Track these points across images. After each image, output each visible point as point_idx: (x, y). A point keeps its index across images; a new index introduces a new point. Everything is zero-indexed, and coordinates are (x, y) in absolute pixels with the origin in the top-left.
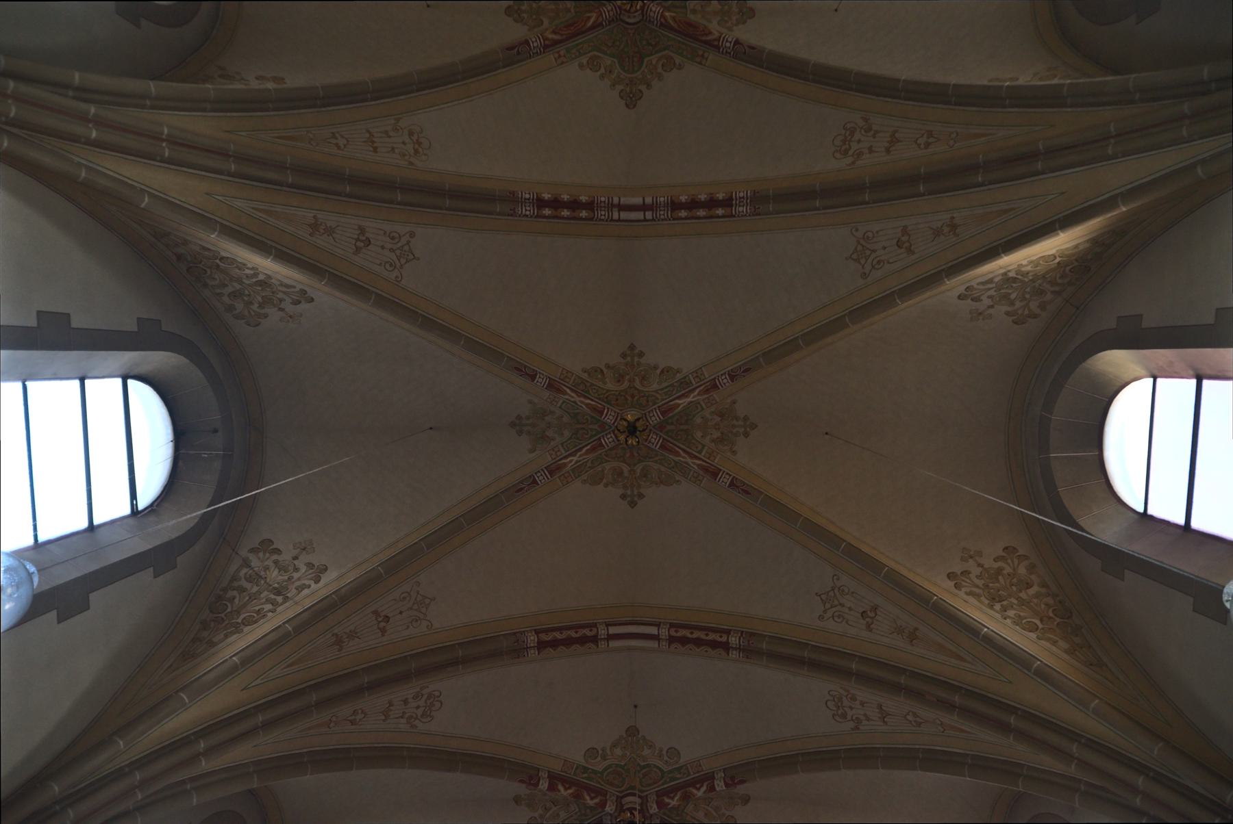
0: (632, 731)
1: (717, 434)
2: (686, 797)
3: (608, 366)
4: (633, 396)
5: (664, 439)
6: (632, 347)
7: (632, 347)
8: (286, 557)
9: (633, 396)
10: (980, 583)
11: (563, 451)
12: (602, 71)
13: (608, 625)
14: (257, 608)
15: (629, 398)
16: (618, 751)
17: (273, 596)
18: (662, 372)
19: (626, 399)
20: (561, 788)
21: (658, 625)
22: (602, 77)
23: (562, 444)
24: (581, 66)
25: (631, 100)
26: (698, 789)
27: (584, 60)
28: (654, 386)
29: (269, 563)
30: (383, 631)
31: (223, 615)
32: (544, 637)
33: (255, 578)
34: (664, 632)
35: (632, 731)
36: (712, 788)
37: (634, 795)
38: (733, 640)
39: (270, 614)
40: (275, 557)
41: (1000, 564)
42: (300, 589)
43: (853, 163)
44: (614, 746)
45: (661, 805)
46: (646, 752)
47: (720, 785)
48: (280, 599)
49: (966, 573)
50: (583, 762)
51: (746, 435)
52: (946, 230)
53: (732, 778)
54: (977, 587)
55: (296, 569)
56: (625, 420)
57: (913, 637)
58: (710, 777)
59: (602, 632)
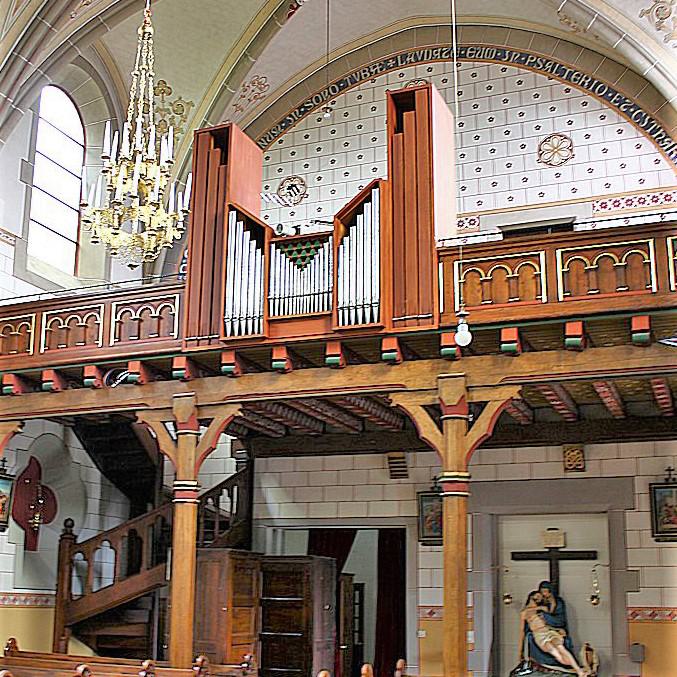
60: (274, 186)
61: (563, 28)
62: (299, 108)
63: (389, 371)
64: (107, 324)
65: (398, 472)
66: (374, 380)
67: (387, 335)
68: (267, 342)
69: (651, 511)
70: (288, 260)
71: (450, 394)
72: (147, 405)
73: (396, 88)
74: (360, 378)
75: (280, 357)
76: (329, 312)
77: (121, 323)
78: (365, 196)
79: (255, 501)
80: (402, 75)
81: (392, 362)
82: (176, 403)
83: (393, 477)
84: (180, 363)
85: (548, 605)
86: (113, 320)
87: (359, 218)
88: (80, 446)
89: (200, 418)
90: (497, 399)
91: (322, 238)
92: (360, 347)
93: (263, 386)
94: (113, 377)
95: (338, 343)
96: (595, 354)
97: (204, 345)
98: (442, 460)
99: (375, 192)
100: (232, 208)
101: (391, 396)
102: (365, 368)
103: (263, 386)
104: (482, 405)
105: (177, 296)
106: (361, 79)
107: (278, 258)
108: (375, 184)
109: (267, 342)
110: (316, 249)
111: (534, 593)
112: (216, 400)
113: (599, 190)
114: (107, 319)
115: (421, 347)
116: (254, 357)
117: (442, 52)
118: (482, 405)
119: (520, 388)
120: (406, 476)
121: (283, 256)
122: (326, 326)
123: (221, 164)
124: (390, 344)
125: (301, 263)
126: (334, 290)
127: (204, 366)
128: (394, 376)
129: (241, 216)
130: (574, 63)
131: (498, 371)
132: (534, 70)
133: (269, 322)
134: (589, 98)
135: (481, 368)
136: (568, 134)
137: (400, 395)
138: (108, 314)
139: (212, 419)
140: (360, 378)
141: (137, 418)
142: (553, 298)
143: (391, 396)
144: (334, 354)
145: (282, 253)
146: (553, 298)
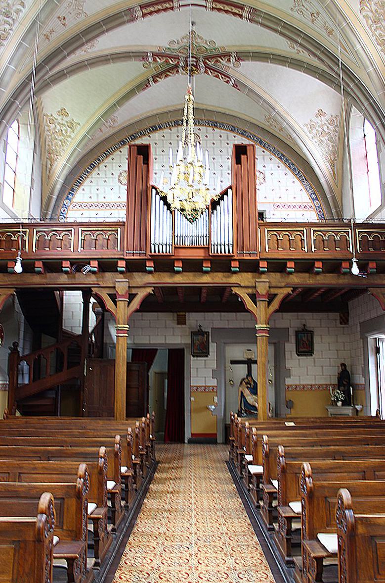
0: (193, 32)
2: (217, 61)
10: (374, 7)
16: (185, 40)
32: (145, 11)
34: (209, 5)
35: (193, 32)
36: (229, 60)
38: (245, 14)
45: (205, 63)
46: (199, 40)
47: (233, 60)
57: (330, 33)
59: (176, 5)
60: (117, 174)
61: (265, 123)
63: (232, 276)
64: (76, 239)
65: (181, 321)
66: (225, 280)
67: (235, 260)
69: (296, 344)
71: (262, 289)
72: (99, 284)
73: (239, 143)
74: (218, 279)
75: (178, 267)
76: (207, 246)
77: (84, 240)
78: (225, 193)
79: (105, 334)
82: (117, 285)
83: (178, 324)
84: (122, 265)
85: (250, 384)
88: (18, 302)
89: (130, 293)
90: (282, 293)
92: (222, 264)
93: (167, 279)
94: (79, 270)
95: (209, 262)
96: (325, 276)
98: (254, 319)
99: (230, 191)
100: (153, 187)
101: (232, 289)
102: (220, 275)
103: (167, 279)
104: (276, 295)
106: (164, 127)
108: (231, 187)
109: (173, 257)
111: (244, 379)
112: (140, 284)
113: (277, 200)
114: (76, 237)
115: (250, 267)
116: (164, 264)
118: (276, 295)
119: (292, 289)
120: (185, 324)
122: (205, 253)
124: (235, 265)
126: (210, 237)
127: (135, 267)
128: (234, 279)
131: (283, 280)
132: (249, 139)
133: (175, 248)
135: (275, 278)
137: (237, 288)
138: (76, 234)
139: (137, 294)
140: (218, 279)
141: (92, 291)
142: (310, 250)
144: (207, 267)
146: (310, 250)
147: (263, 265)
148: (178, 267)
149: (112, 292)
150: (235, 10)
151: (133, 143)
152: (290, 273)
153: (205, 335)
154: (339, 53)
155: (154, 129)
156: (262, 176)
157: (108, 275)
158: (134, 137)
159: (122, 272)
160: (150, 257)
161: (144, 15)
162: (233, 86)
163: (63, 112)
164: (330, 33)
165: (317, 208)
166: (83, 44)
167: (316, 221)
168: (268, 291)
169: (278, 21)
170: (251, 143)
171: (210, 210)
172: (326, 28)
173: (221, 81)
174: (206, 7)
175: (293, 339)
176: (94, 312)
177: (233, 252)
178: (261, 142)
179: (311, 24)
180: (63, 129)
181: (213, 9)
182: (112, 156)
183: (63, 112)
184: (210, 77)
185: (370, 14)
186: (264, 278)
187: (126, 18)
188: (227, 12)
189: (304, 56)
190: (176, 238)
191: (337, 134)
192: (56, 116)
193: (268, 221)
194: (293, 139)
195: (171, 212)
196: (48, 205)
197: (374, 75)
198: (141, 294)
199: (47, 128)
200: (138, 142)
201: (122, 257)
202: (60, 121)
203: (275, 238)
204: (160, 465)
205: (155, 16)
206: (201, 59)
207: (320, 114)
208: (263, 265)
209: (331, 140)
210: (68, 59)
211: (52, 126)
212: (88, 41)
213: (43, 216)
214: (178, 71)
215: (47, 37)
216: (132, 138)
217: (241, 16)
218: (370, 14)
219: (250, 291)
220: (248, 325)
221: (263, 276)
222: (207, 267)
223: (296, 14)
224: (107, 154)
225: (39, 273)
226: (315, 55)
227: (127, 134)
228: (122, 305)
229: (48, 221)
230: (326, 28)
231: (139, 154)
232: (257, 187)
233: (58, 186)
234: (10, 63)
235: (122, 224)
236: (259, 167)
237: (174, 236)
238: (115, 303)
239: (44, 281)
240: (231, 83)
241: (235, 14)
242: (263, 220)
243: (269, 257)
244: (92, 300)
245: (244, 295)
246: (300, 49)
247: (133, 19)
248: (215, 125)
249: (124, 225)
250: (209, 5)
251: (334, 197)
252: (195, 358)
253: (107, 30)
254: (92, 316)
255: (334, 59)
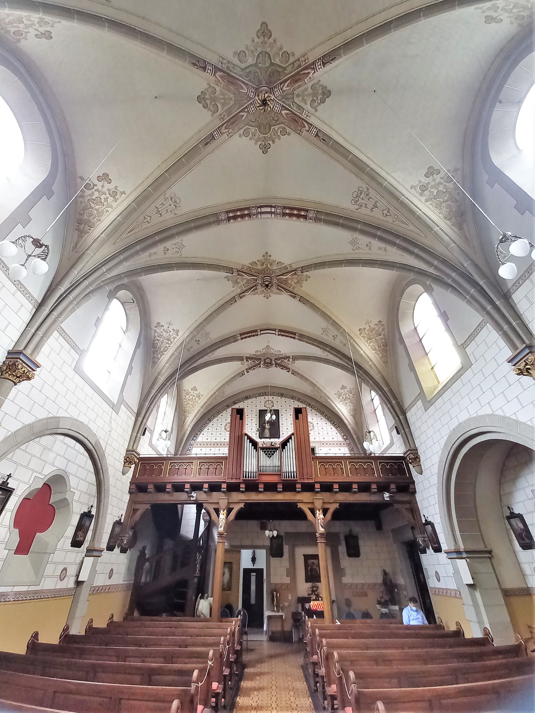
0: (268, 346)
1: (296, 281)
2: (282, 361)
3: (258, 261)
4: (267, 271)
5: (278, 285)
6: (267, 253)
7: (267, 253)
8: (165, 327)
9: (267, 271)
10: (367, 333)
11: (244, 288)
12: (251, 135)
13: (261, 331)
14: (165, 346)
15: (266, 271)
16: (264, 350)
17: (168, 342)
18: (277, 263)
19: (265, 272)
20: (249, 360)
21: (275, 330)
22: (251, 139)
23: (243, 285)
24: (240, 136)
25: (265, 149)
26: (285, 360)
27: (241, 131)
28: (275, 267)
29: (162, 330)
30: (199, 344)
31: (157, 349)
32: (242, 337)
33: (160, 336)
35: (268, 346)
36: (289, 360)
37: (268, 359)
38: (296, 337)
39: (169, 348)
40: (163, 328)
41: (375, 326)
42: (174, 338)
43: (358, 209)
44: (263, 349)
46: (272, 350)
47: (291, 360)
48: (170, 342)
49: (365, 328)
50: (255, 354)
51: (306, 280)
52: (383, 249)
53: (294, 359)
54: (366, 334)
55: (170, 332)
56: (265, 284)
58: (289, 357)
59: (259, 333)
60: (224, 425)
62: (233, 402)
67: (299, 483)
68: (257, 481)
70: (265, 454)
75: (261, 488)
76: (280, 473)
77: (201, 469)
78: (290, 438)
80: (265, 398)
81: (299, 492)
84: (224, 486)
86: (198, 467)
87: (288, 444)
91: (277, 449)
95: (281, 484)
97: (234, 480)
99: (293, 436)
100: (246, 434)
101: (298, 504)
105: (224, 461)
106: (252, 397)
107: (261, 453)
108: (293, 434)
110: (274, 452)
115: (308, 488)
117: (276, 394)
121: (263, 452)
123: (240, 420)
124: (298, 486)
125: (270, 455)
126: (281, 466)
127: (233, 488)
129: (249, 438)
130: (313, 403)
134: (317, 413)
136: (312, 422)
139: (233, 508)
143: (298, 504)
144: (280, 487)
145: (262, 451)
147: (317, 486)
148: (261, 488)
149: (216, 506)
150: (291, 335)
151: (233, 407)
152: (336, 492)
153: (280, 539)
154: (352, 356)
155: (247, 398)
156: (312, 425)
157: (214, 493)
158: (235, 403)
159: (224, 492)
160: (242, 481)
161: (242, 339)
162: (292, 373)
163: (195, 389)
164: (345, 345)
165: (349, 445)
166: (208, 354)
167: (349, 455)
168: (322, 506)
169: (315, 340)
170: (305, 406)
171: (281, 449)
172: (342, 343)
173: (285, 371)
174: (275, 334)
175: (343, 543)
176: (204, 520)
177: (296, 478)
178: (309, 405)
179: (333, 341)
180: (194, 398)
181: (279, 335)
182: (221, 414)
183: (195, 389)
184: (279, 369)
185: (365, 335)
186: (319, 496)
187: (232, 340)
188: (287, 336)
189: (331, 357)
190: (260, 467)
191: (355, 399)
192: (190, 391)
193: (318, 455)
194: (329, 403)
195: (256, 451)
196: (180, 447)
197: (373, 366)
198: (236, 508)
199: (184, 397)
200: (237, 406)
201: (225, 481)
202: (192, 393)
203: (324, 467)
204: (246, 670)
205: (248, 339)
206: (273, 360)
207: (343, 387)
208: (317, 486)
209: (351, 402)
210: (200, 360)
211: (187, 397)
212: (210, 352)
213: (176, 454)
214: (260, 367)
215: (188, 350)
216: (233, 403)
217: (294, 338)
218: (365, 335)
219: (310, 506)
220: (310, 531)
221: (318, 495)
222: (280, 487)
223: (324, 336)
224: (219, 413)
225: (168, 492)
226: (337, 357)
227: (231, 401)
228: (223, 516)
229: (178, 456)
230: (342, 343)
231: (237, 414)
232: (310, 432)
233: (188, 432)
234: (166, 363)
235: (225, 458)
236: (310, 419)
237: (258, 467)
238: (218, 516)
239: (171, 498)
240: (290, 372)
241: (291, 337)
242: (314, 455)
243: (321, 480)
244: (203, 511)
245: (305, 508)
246: (329, 354)
247: (236, 341)
248: (282, 395)
249: (227, 459)
250: (277, 333)
251: (358, 438)
252: (274, 558)
253: (222, 346)
254: (202, 523)
255: (350, 359)
